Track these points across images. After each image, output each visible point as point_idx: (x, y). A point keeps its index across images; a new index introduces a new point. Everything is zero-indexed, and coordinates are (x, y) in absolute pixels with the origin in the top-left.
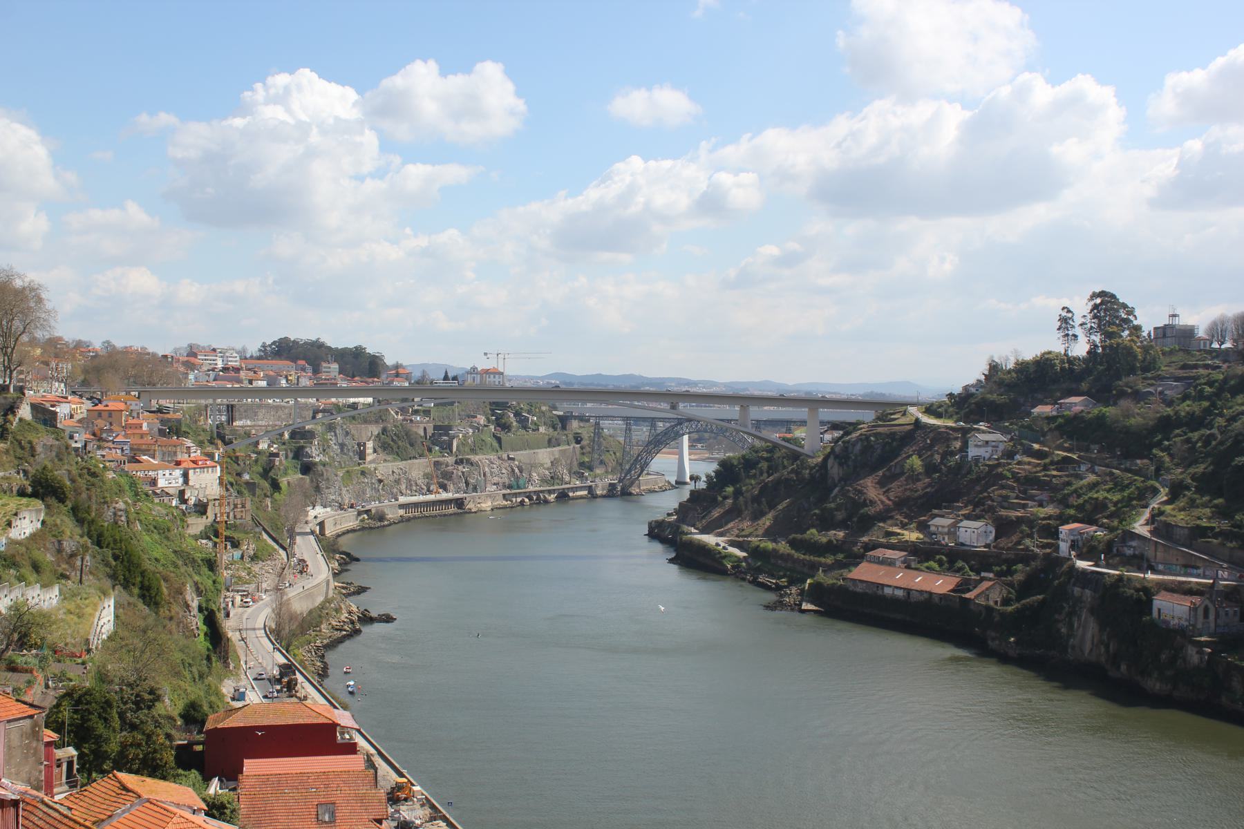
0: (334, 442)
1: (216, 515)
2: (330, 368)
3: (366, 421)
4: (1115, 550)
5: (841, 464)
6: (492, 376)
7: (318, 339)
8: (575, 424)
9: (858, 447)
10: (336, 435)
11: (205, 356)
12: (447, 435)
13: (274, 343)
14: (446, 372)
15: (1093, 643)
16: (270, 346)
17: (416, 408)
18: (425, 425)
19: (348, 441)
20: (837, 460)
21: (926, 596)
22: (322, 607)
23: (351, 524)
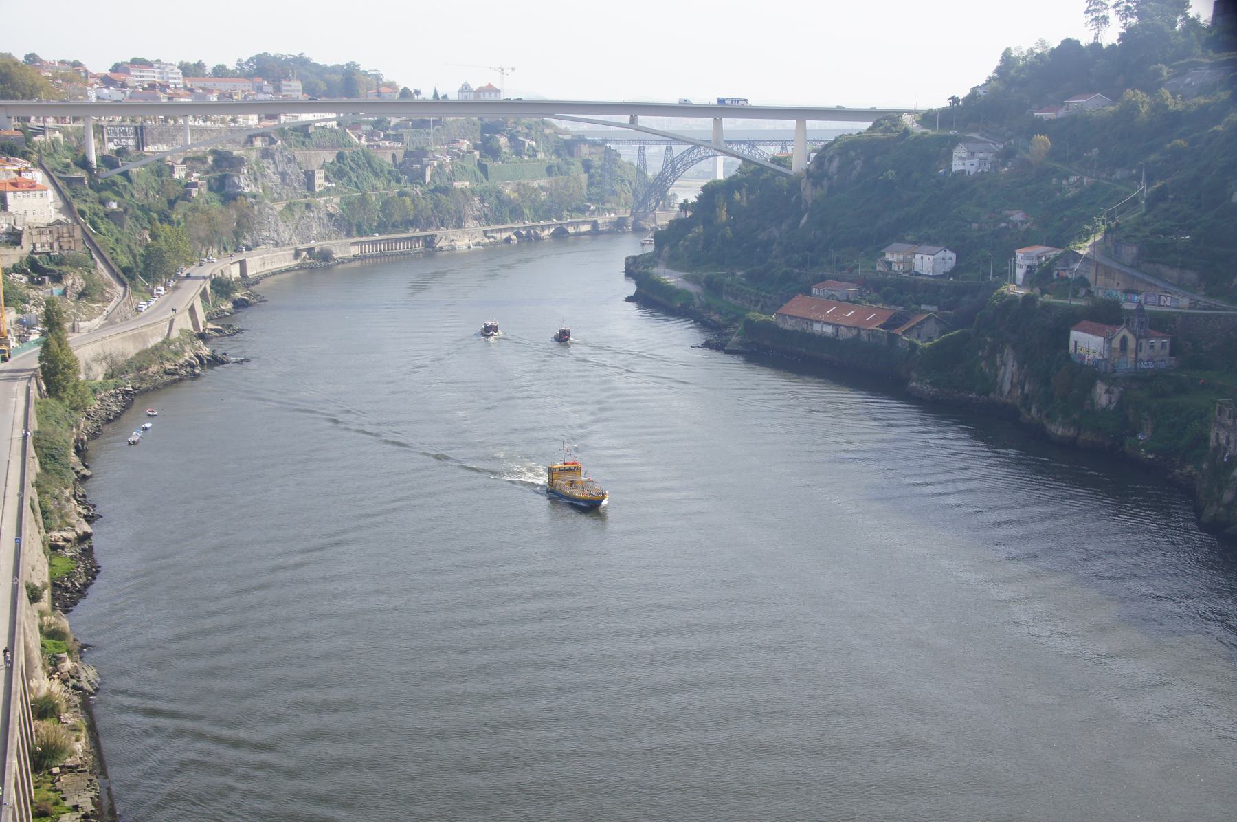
0: (273, 170)
1: (34, 245)
2: (290, 86)
3: (319, 147)
4: (1055, 275)
5: (814, 185)
6: (487, 94)
7: (302, 54)
8: (585, 149)
9: (835, 163)
10: (274, 163)
11: (140, 72)
12: (420, 162)
13: (252, 59)
14: (435, 90)
15: (1012, 383)
16: (247, 63)
17: (390, 132)
18: (395, 152)
19: (291, 169)
20: (811, 180)
21: (854, 332)
22: (156, 348)
23: (287, 264)
